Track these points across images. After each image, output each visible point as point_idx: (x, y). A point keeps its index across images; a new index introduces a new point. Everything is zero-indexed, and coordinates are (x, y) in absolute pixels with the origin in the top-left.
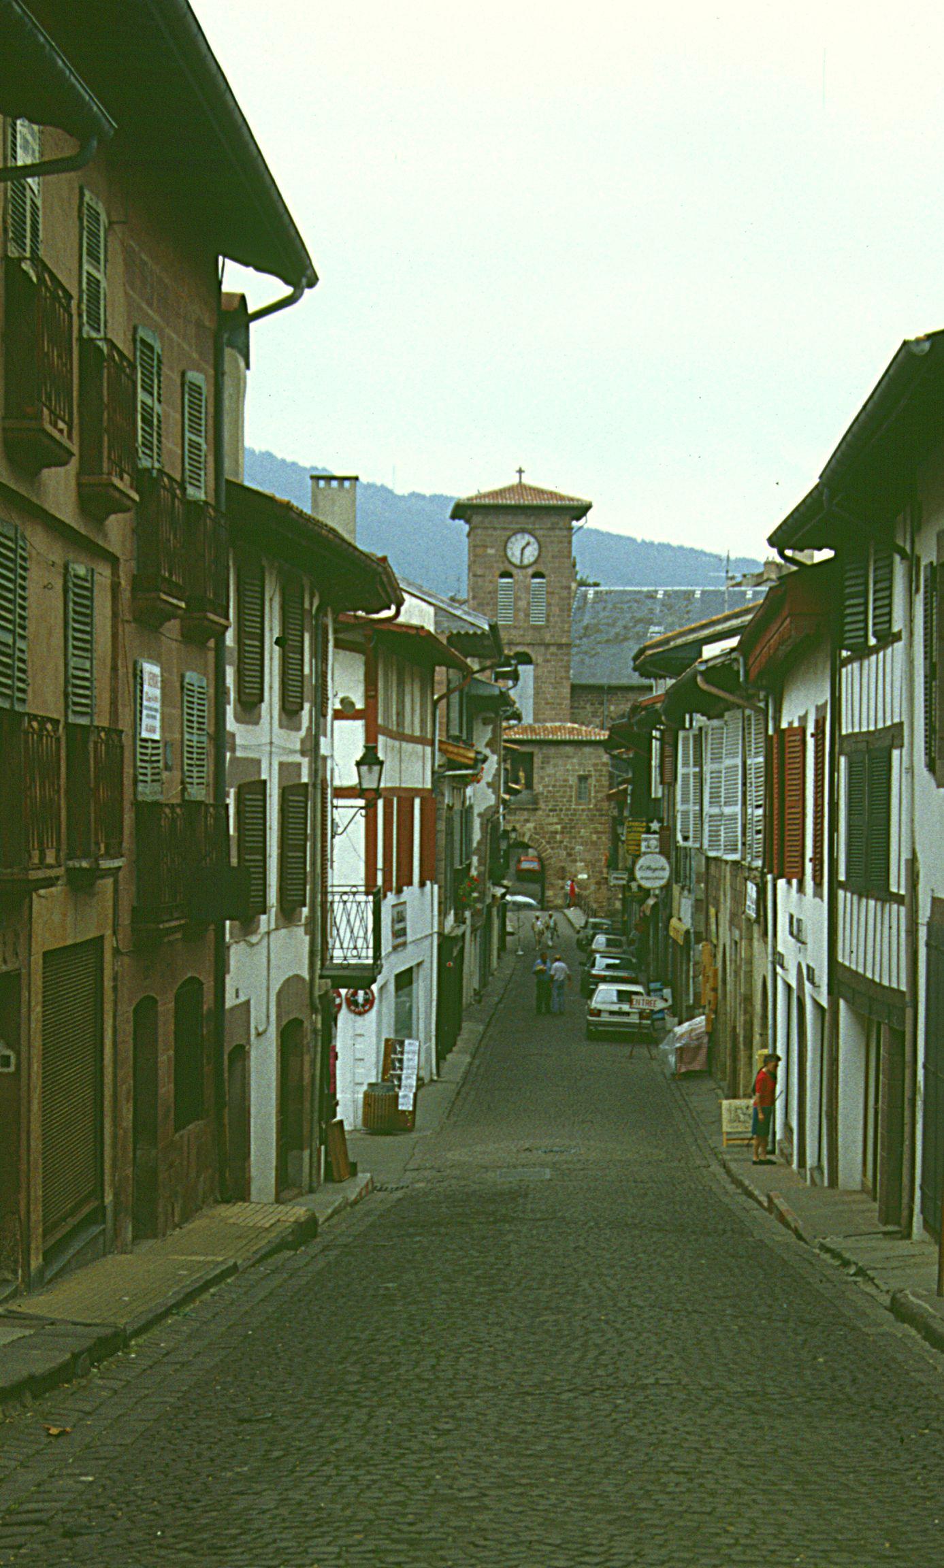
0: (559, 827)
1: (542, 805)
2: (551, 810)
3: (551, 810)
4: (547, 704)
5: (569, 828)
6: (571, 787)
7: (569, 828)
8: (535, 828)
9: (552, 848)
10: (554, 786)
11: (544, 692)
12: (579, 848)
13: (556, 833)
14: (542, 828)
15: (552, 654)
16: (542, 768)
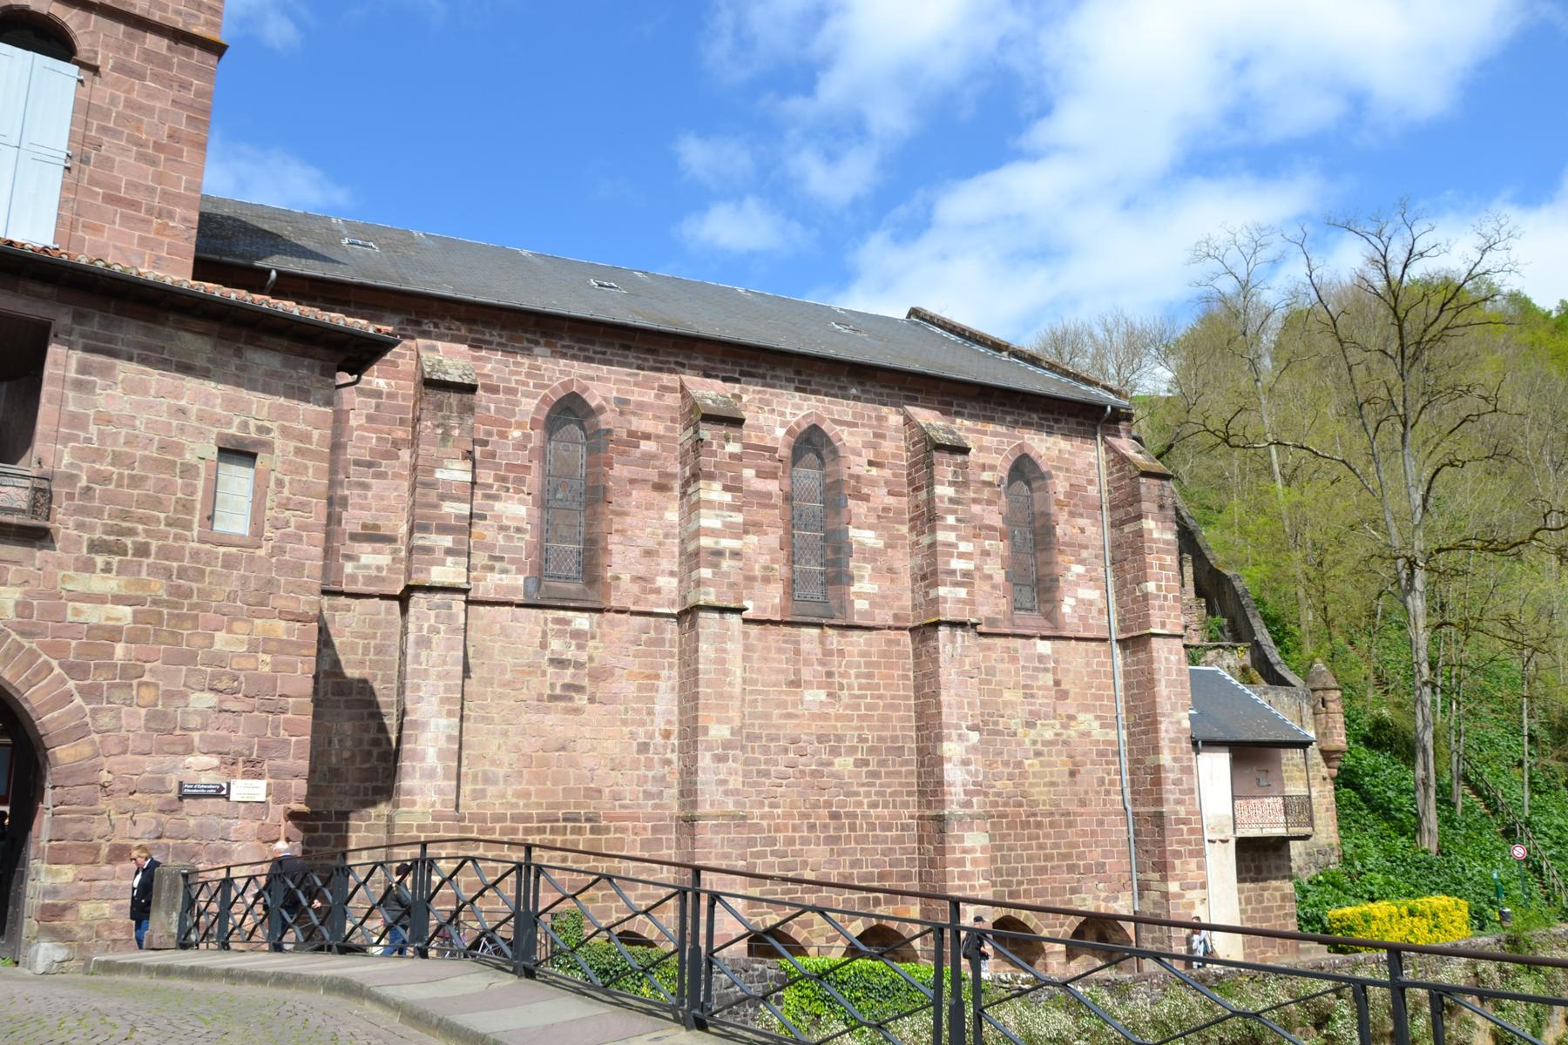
0: (128, 610)
1: (63, 522)
2: (95, 547)
3: (95, 547)
4: (111, 199)
5: (169, 618)
6: (188, 471)
7: (169, 618)
8: (23, 607)
9: (89, 693)
10: (117, 459)
11: (107, 163)
12: (203, 700)
13: (114, 634)
14: (56, 614)
15: (149, 56)
16: (79, 385)
